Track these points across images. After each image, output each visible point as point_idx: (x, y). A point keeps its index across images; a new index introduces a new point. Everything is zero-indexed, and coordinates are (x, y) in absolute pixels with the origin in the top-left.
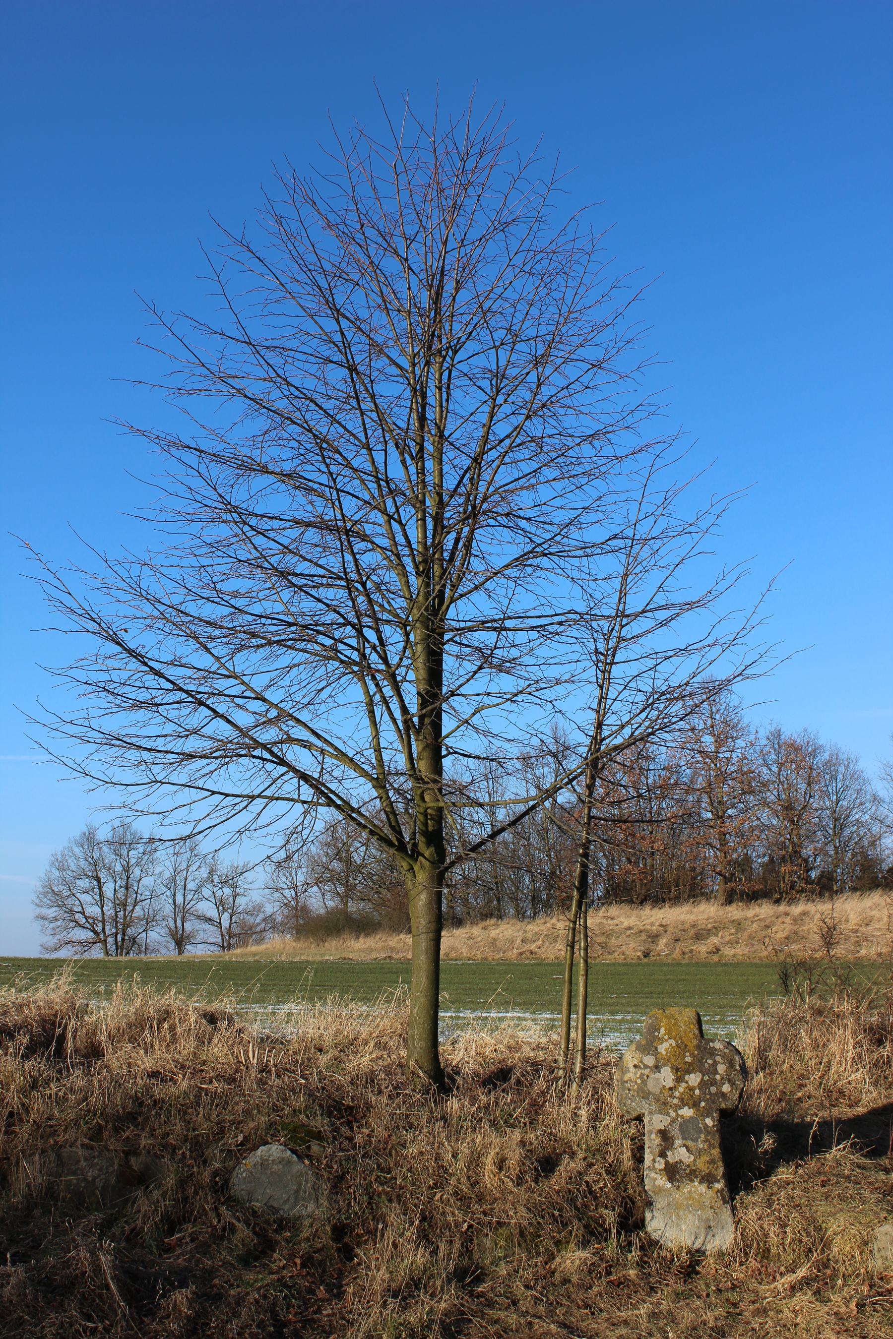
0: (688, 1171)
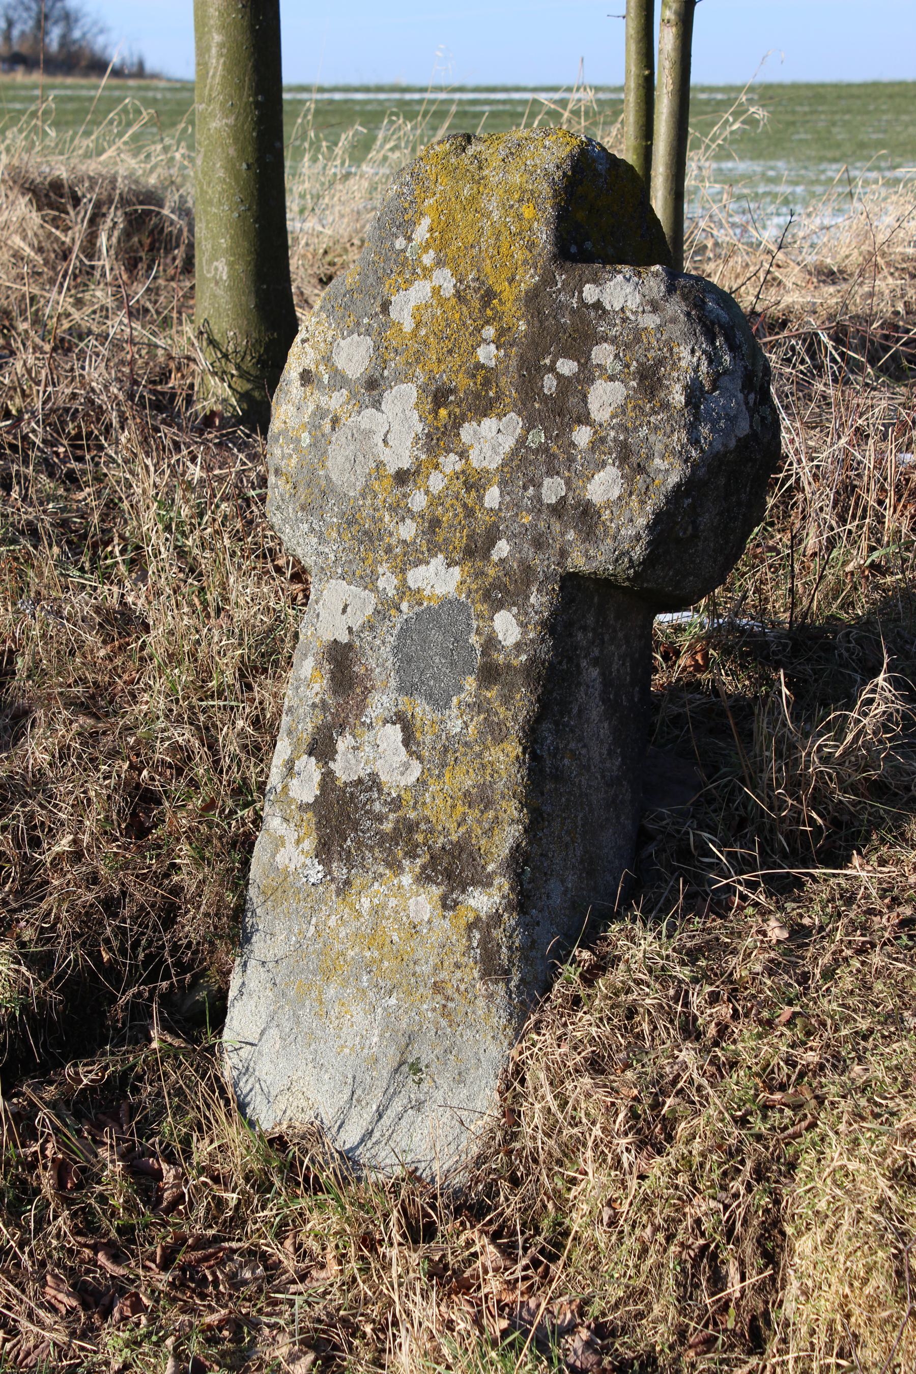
0: (388, 827)
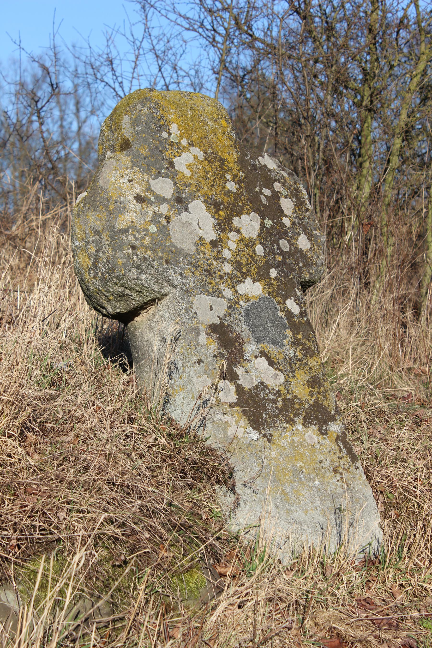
0: (280, 404)
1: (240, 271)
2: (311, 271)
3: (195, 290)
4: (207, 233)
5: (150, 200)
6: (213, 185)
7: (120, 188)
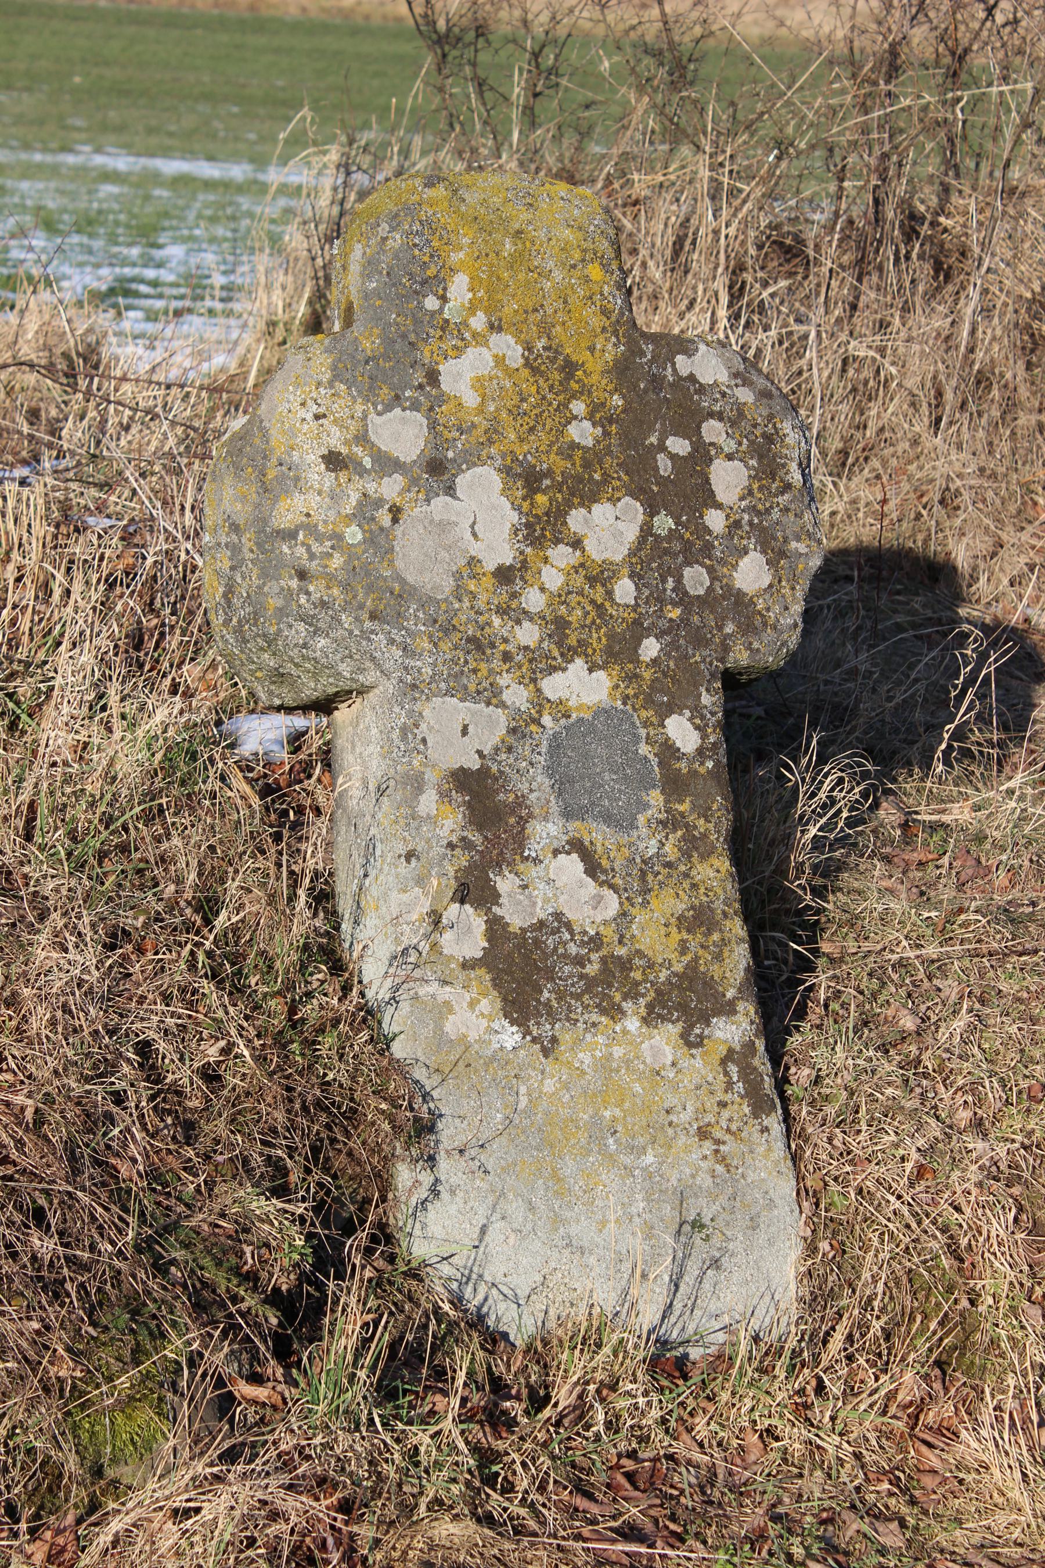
0: (592, 969)
1: (559, 644)
2: (756, 645)
3: (433, 686)
4: (490, 548)
5: (360, 464)
6: (532, 429)
7: (293, 433)
